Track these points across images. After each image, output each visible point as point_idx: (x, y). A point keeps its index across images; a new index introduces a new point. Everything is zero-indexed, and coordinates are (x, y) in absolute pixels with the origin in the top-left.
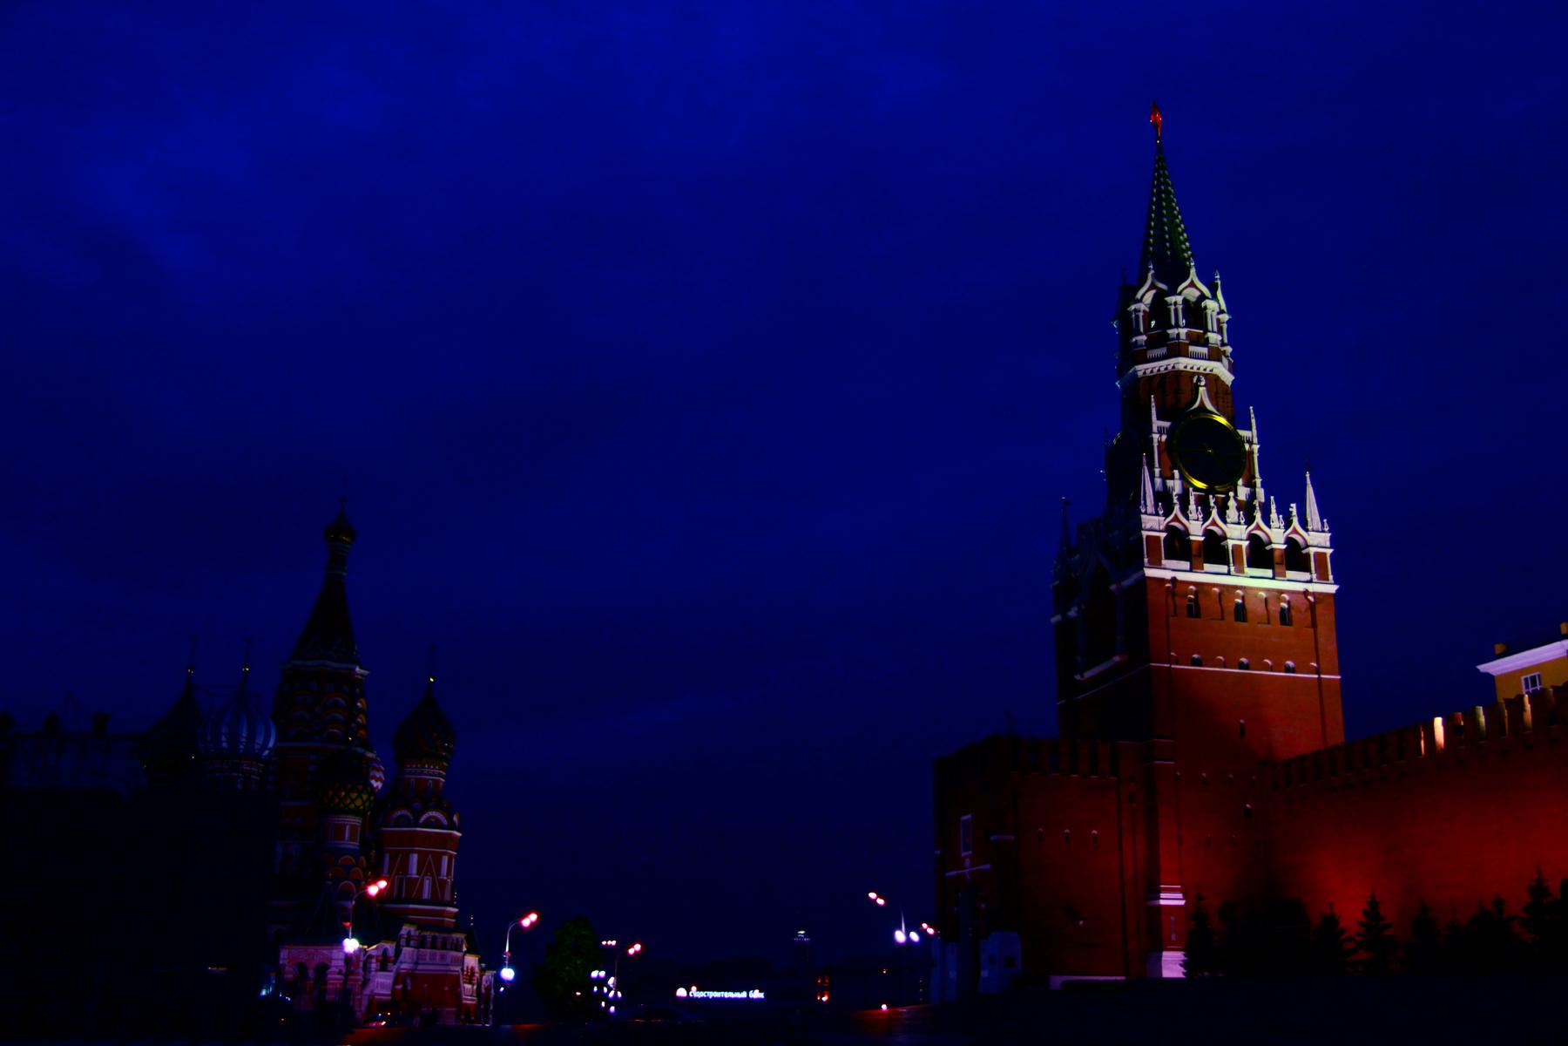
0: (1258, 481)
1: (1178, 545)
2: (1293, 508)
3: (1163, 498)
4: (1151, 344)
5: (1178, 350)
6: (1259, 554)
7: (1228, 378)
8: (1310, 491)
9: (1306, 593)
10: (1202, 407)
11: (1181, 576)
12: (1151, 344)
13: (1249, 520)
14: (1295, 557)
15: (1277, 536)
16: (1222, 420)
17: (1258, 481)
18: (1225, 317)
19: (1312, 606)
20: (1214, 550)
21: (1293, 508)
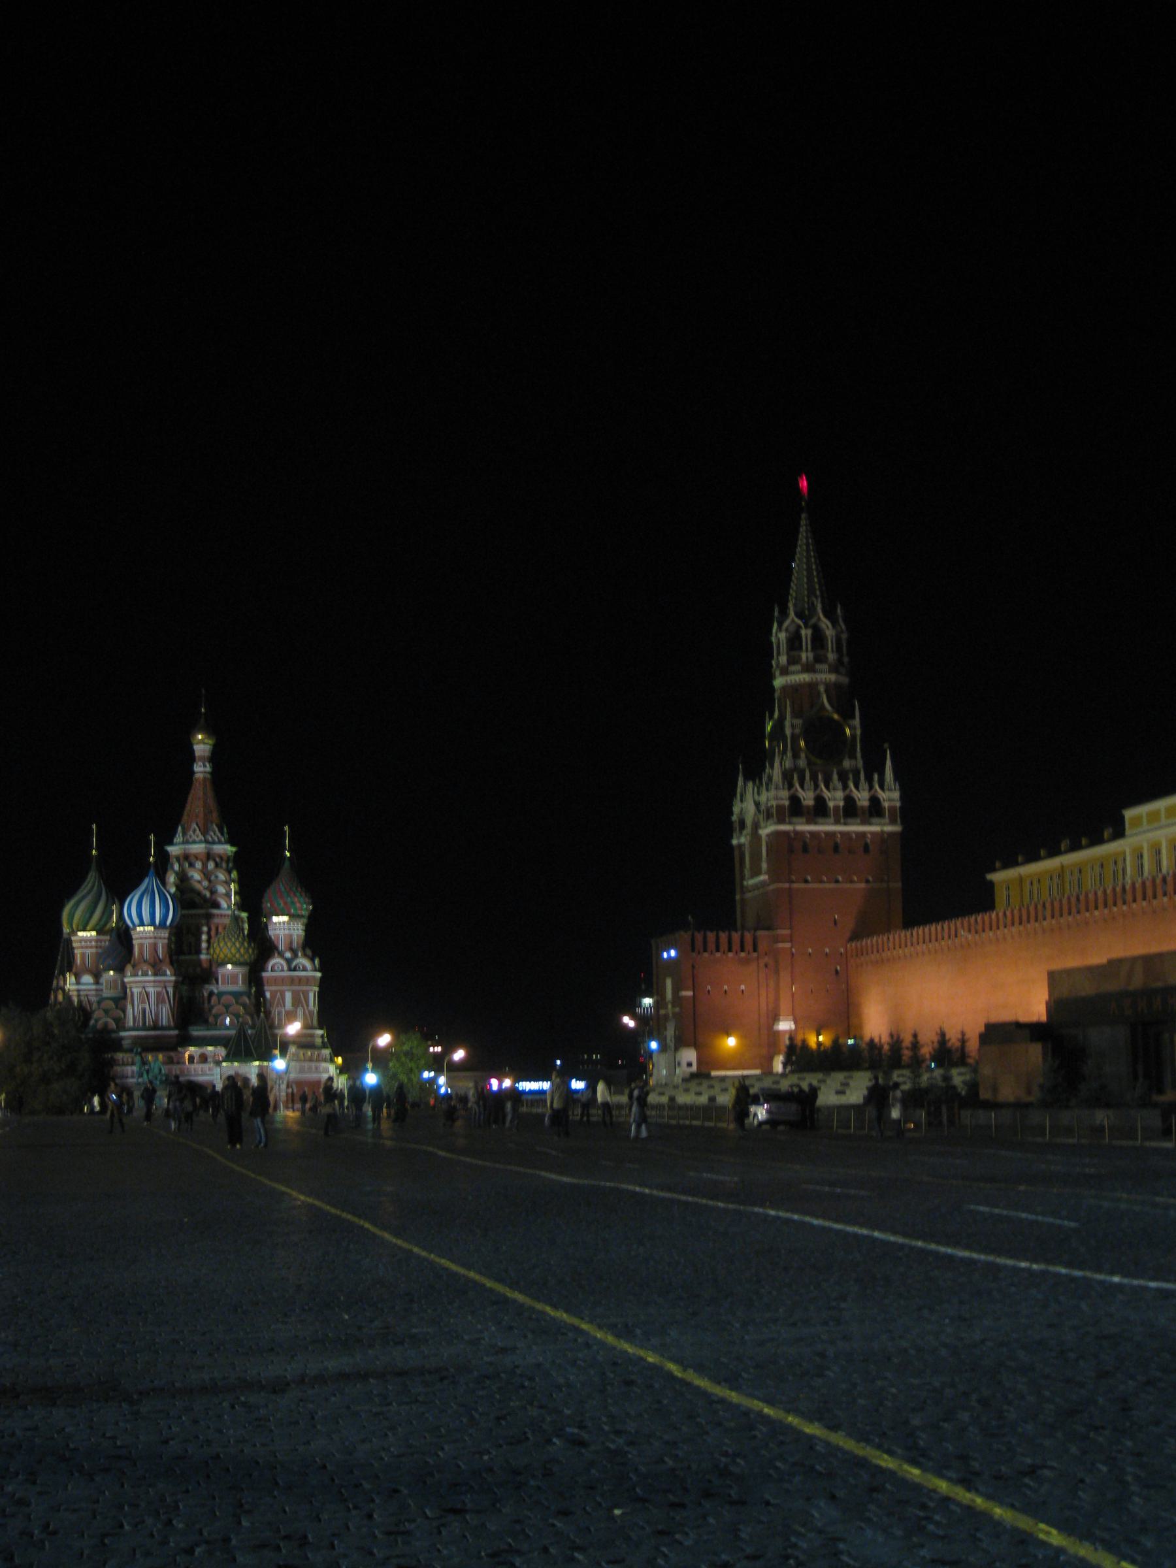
0: (859, 755)
1: (796, 808)
2: (876, 777)
3: (787, 777)
5: (809, 668)
6: (850, 810)
7: (845, 680)
8: (889, 763)
9: (882, 832)
11: (800, 828)
13: (845, 787)
14: (875, 810)
15: (862, 797)
16: (836, 716)
17: (859, 755)
18: (844, 636)
20: (820, 810)
21: (876, 777)
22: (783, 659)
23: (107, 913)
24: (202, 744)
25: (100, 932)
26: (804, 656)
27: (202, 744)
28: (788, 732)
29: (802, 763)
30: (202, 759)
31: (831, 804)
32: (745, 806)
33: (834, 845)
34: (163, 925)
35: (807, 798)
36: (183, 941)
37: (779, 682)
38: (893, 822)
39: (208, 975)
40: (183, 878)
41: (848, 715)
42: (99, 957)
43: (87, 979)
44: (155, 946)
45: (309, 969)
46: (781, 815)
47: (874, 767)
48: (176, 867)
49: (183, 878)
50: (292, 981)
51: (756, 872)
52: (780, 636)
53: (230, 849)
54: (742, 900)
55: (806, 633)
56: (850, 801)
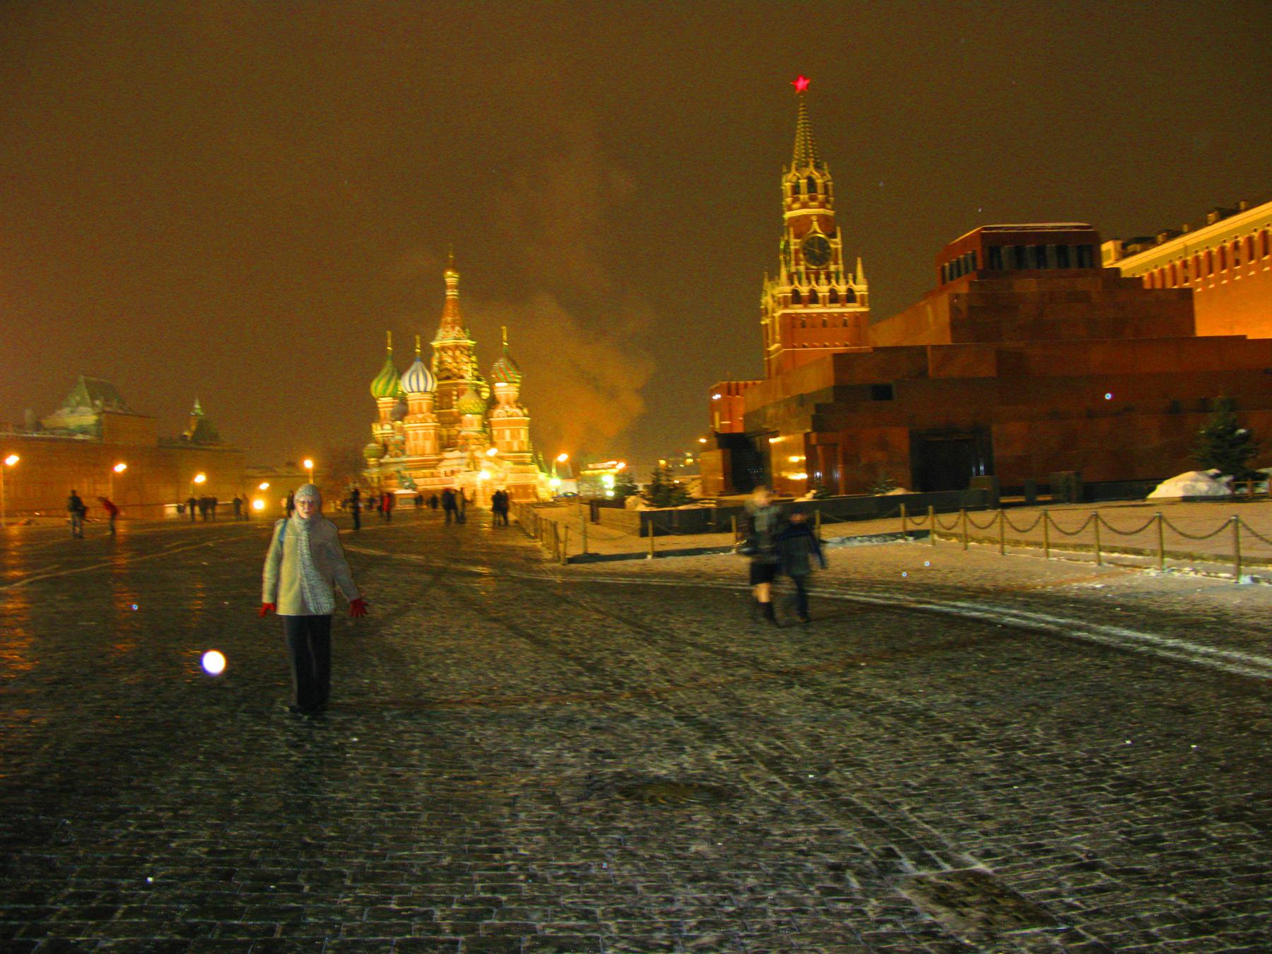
0: (840, 262)
1: (796, 298)
2: (850, 276)
4: (794, 202)
5: (804, 206)
6: (834, 298)
7: (830, 213)
10: (815, 232)
12: (794, 202)
13: (829, 283)
14: (851, 297)
15: (842, 289)
17: (840, 262)
19: (857, 318)
20: (813, 298)
21: (850, 276)
22: (789, 200)
23: (396, 384)
24: (451, 277)
25: (394, 397)
26: (801, 197)
27: (451, 277)
28: (792, 247)
29: (802, 268)
30: (452, 287)
31: (820, 295)
32: (767, 300)
33: (824, 322)
34: (425, 391)
35: (804, 290)
36: (442, 402)
37: (788, 215)
38: (863, 305)
39: (457, 420)
40: (441, 362)
41: (833, 235)
42: (393, 414)
43: (387, 427)
44: (420, 404)
45: (520, 415)
46: (785, 302)
47: (850, 269)
48: (437, 355)
49: (441, 362)
50: (509, 423)
51: (774, 342)
52: (787, 186)
53: (470, 343)
54: (769, 361)
55: (803, 182)
56: (833, 292)
